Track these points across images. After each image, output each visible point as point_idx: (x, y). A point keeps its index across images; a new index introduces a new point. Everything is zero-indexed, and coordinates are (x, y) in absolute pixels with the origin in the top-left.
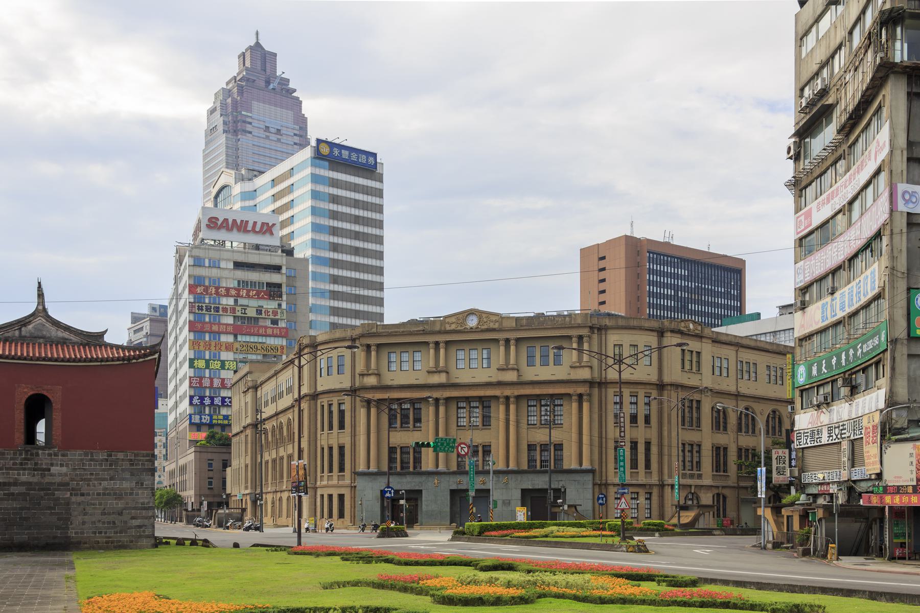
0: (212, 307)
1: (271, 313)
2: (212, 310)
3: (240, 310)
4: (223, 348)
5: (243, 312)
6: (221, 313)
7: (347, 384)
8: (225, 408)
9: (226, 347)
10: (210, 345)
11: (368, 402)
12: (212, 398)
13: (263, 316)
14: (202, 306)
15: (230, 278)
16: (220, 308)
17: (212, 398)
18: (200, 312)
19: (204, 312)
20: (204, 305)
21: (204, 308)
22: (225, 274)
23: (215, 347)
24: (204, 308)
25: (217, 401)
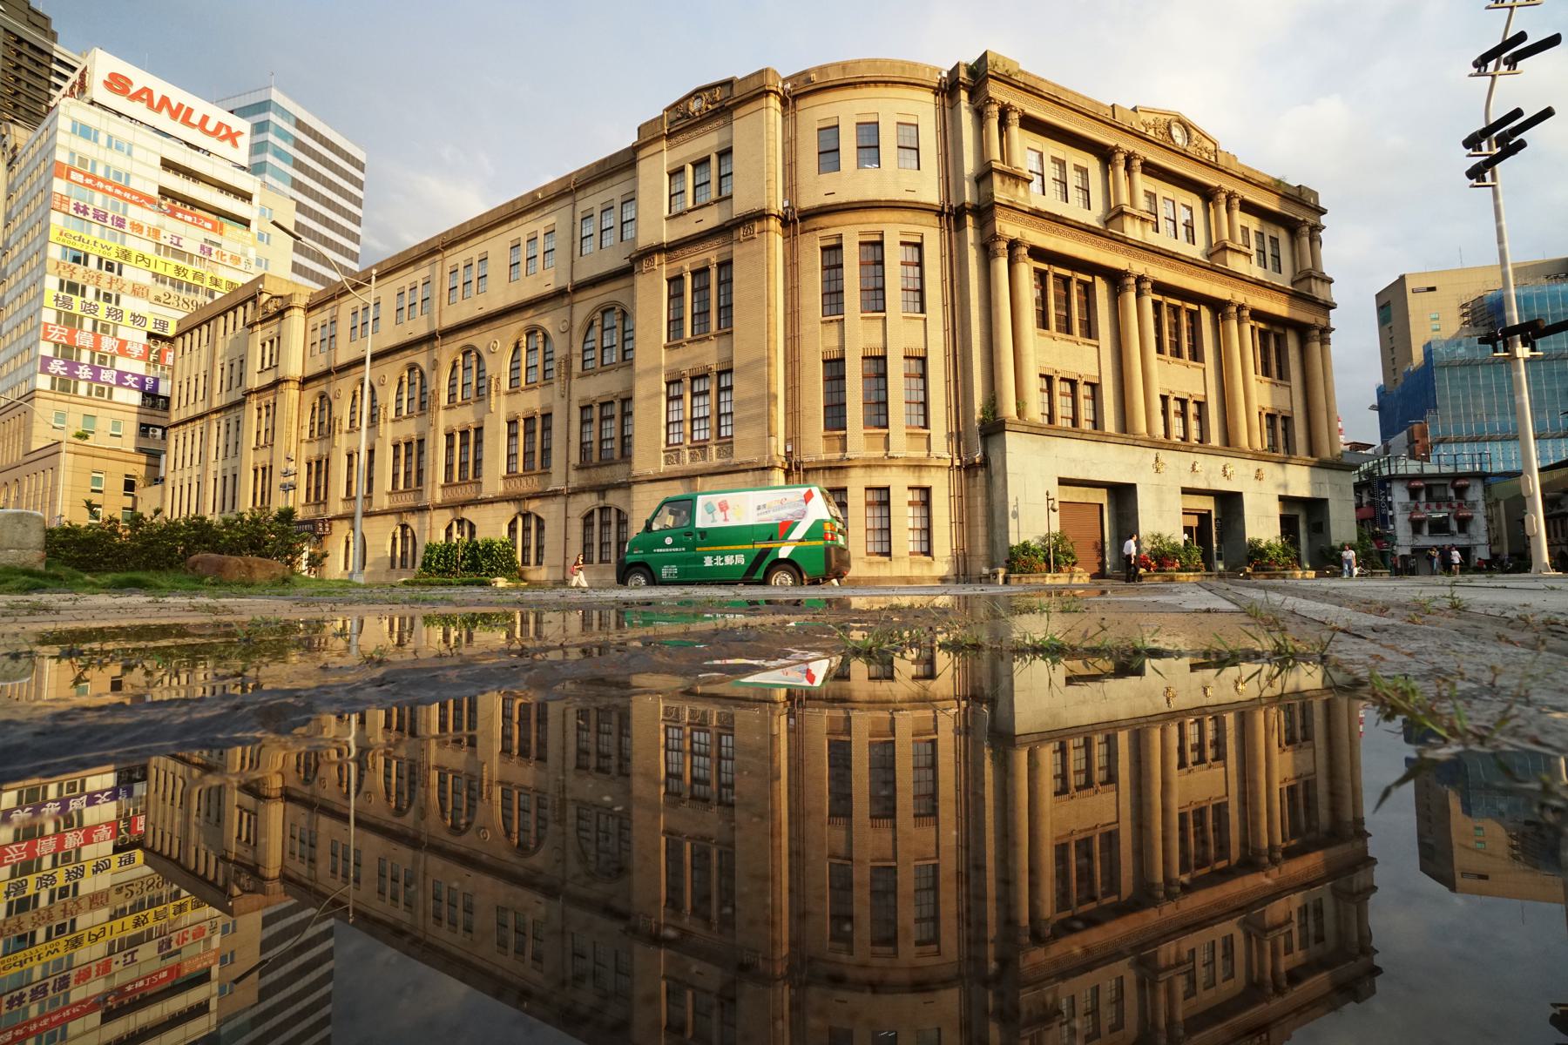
0: (110, 216)
1: (227, 258)
2: (109, 219)
3: (169, 237)
4: (128, 289)
5: (175, 241)
6: (127, 229)
7: (931, 194)
8: (125, 391)
9: (134, 290)
10: (99, 277)
11: (1013, 245)
12: (96, 372)
13: (214, 258)
14: (85, 207)
15: (151, 179)
16: (128, 222)
17: (96, 372)
18: (81, 215)
19: (90, 217)
20: (91, 208)
21: (91, 212)
22: (136, 168)
23: (111, 283)
24: (91, 212)
25: (107, 376)
